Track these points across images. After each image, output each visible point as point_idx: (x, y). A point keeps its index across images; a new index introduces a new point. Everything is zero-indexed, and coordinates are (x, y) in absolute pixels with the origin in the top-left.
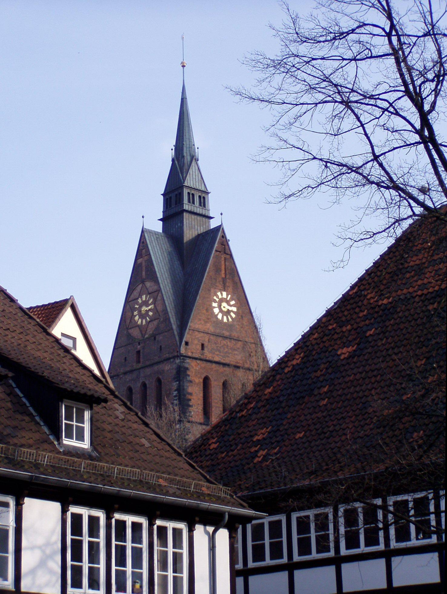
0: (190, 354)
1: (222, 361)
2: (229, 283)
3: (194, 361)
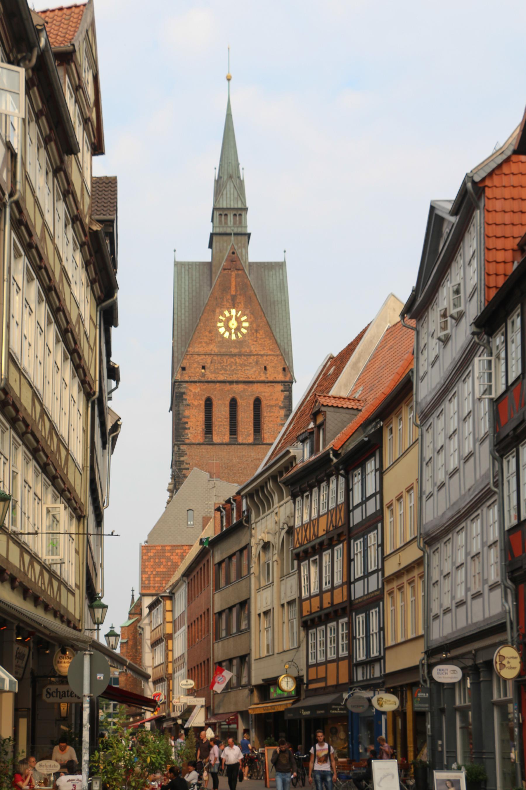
0: (187, 379)
1: (229, 379)
2: (240, 299)
3: (193, 384)
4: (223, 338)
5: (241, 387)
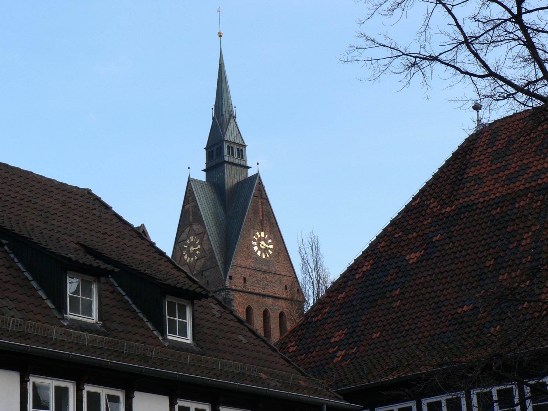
0: (234, 287)
1: (262, 293)
2: (266, 224)
4: (257, 255)
5: (270, 301)
